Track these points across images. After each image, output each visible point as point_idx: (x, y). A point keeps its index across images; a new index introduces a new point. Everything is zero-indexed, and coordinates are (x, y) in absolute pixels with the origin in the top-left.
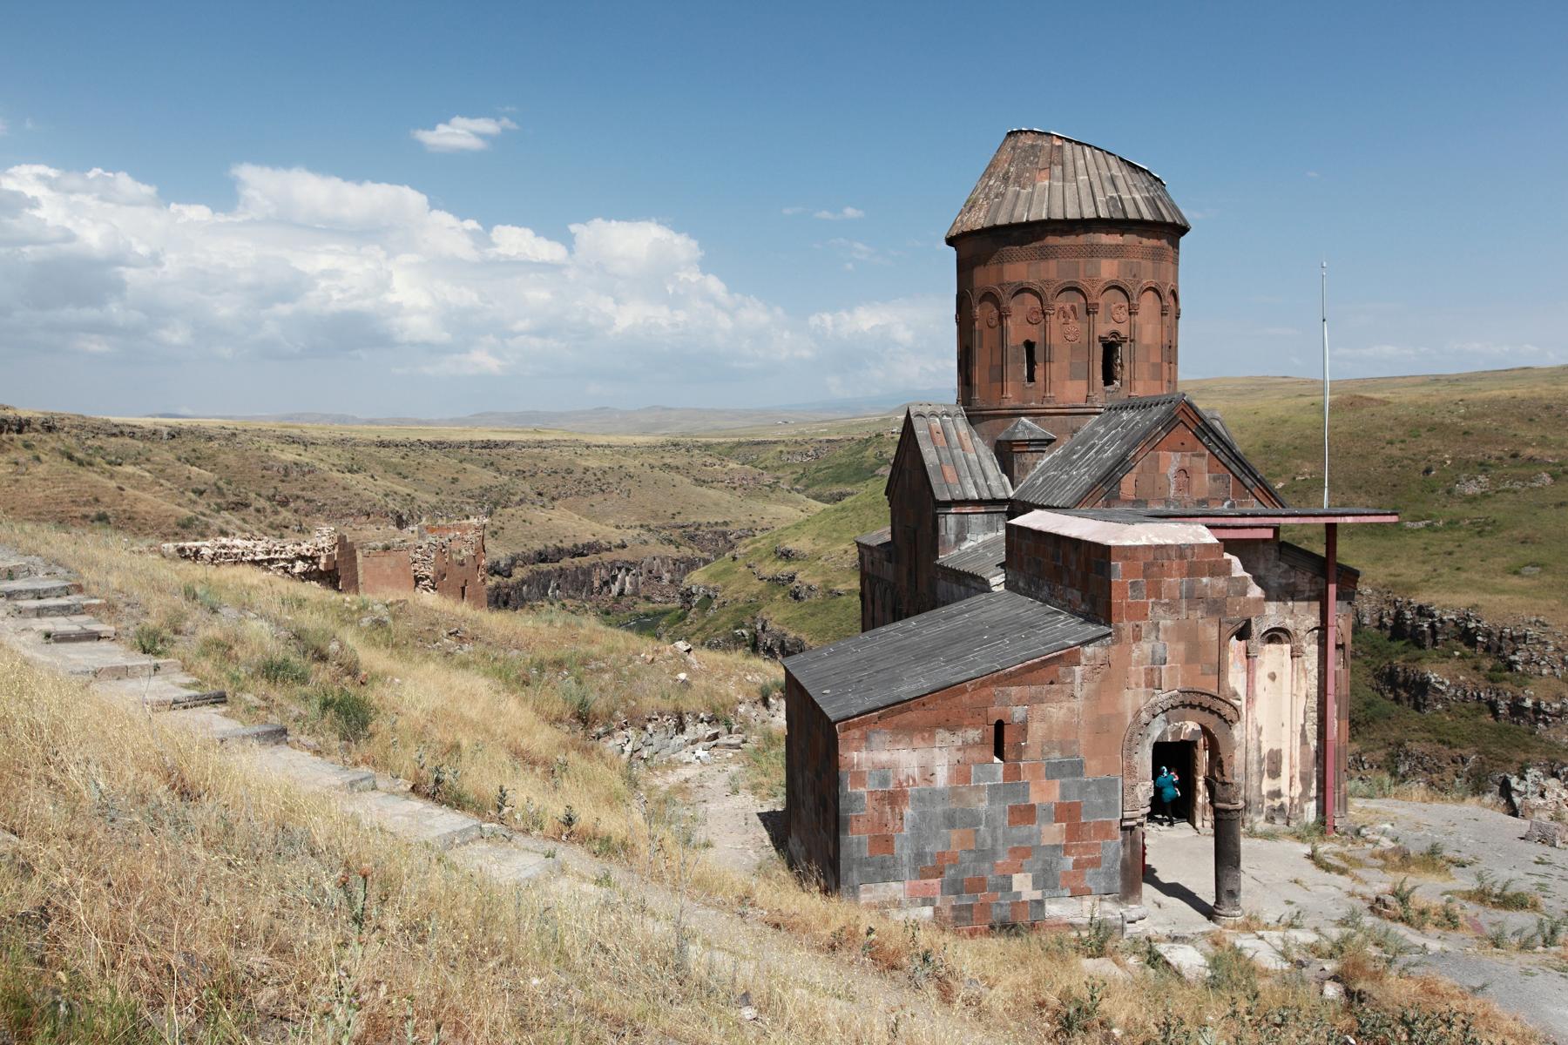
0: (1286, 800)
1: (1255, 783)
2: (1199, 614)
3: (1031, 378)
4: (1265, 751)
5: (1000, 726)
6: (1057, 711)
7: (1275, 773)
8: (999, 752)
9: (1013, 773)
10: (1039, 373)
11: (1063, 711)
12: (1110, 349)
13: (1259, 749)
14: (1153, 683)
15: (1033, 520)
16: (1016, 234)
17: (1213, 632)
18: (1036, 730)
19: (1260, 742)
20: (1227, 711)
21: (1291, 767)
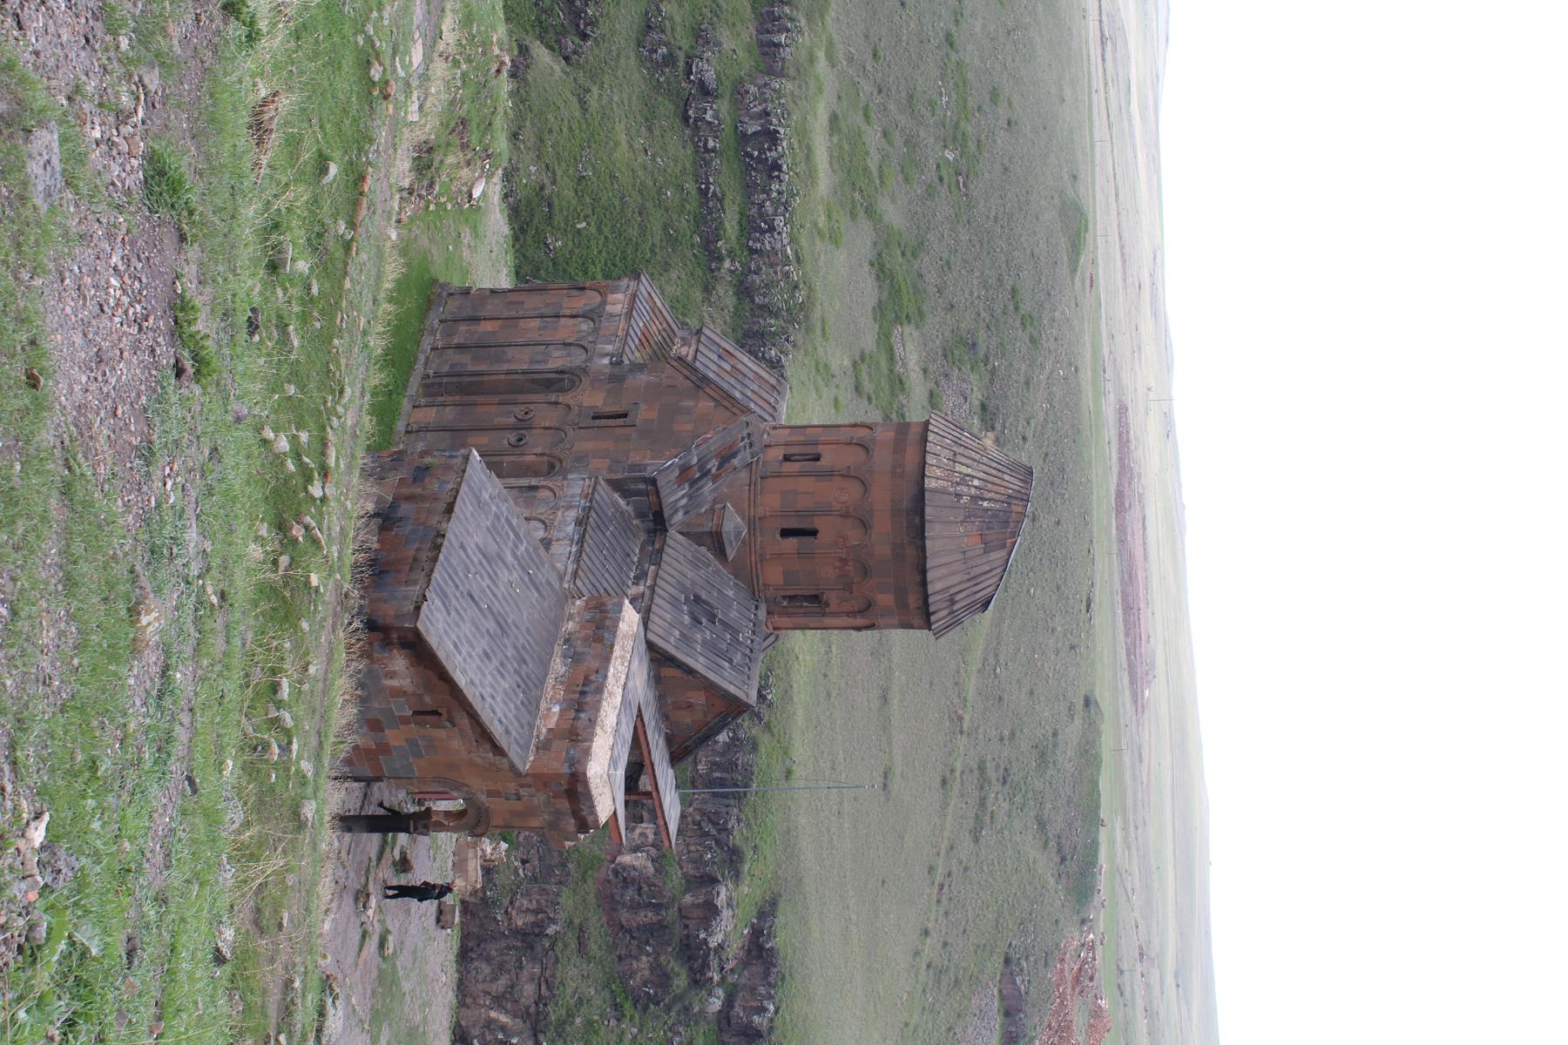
3: (785, 533)
5: (436, 713)
6: (456, 744)
8: (416, 713)
9: (405, 721)
10: (792, 543)
12: (815, 598)
14: (490, 794)
15: (630, 618)
16: (917, 520)
17: (535, 823)
18: (441, 734)
20: (479, 830)
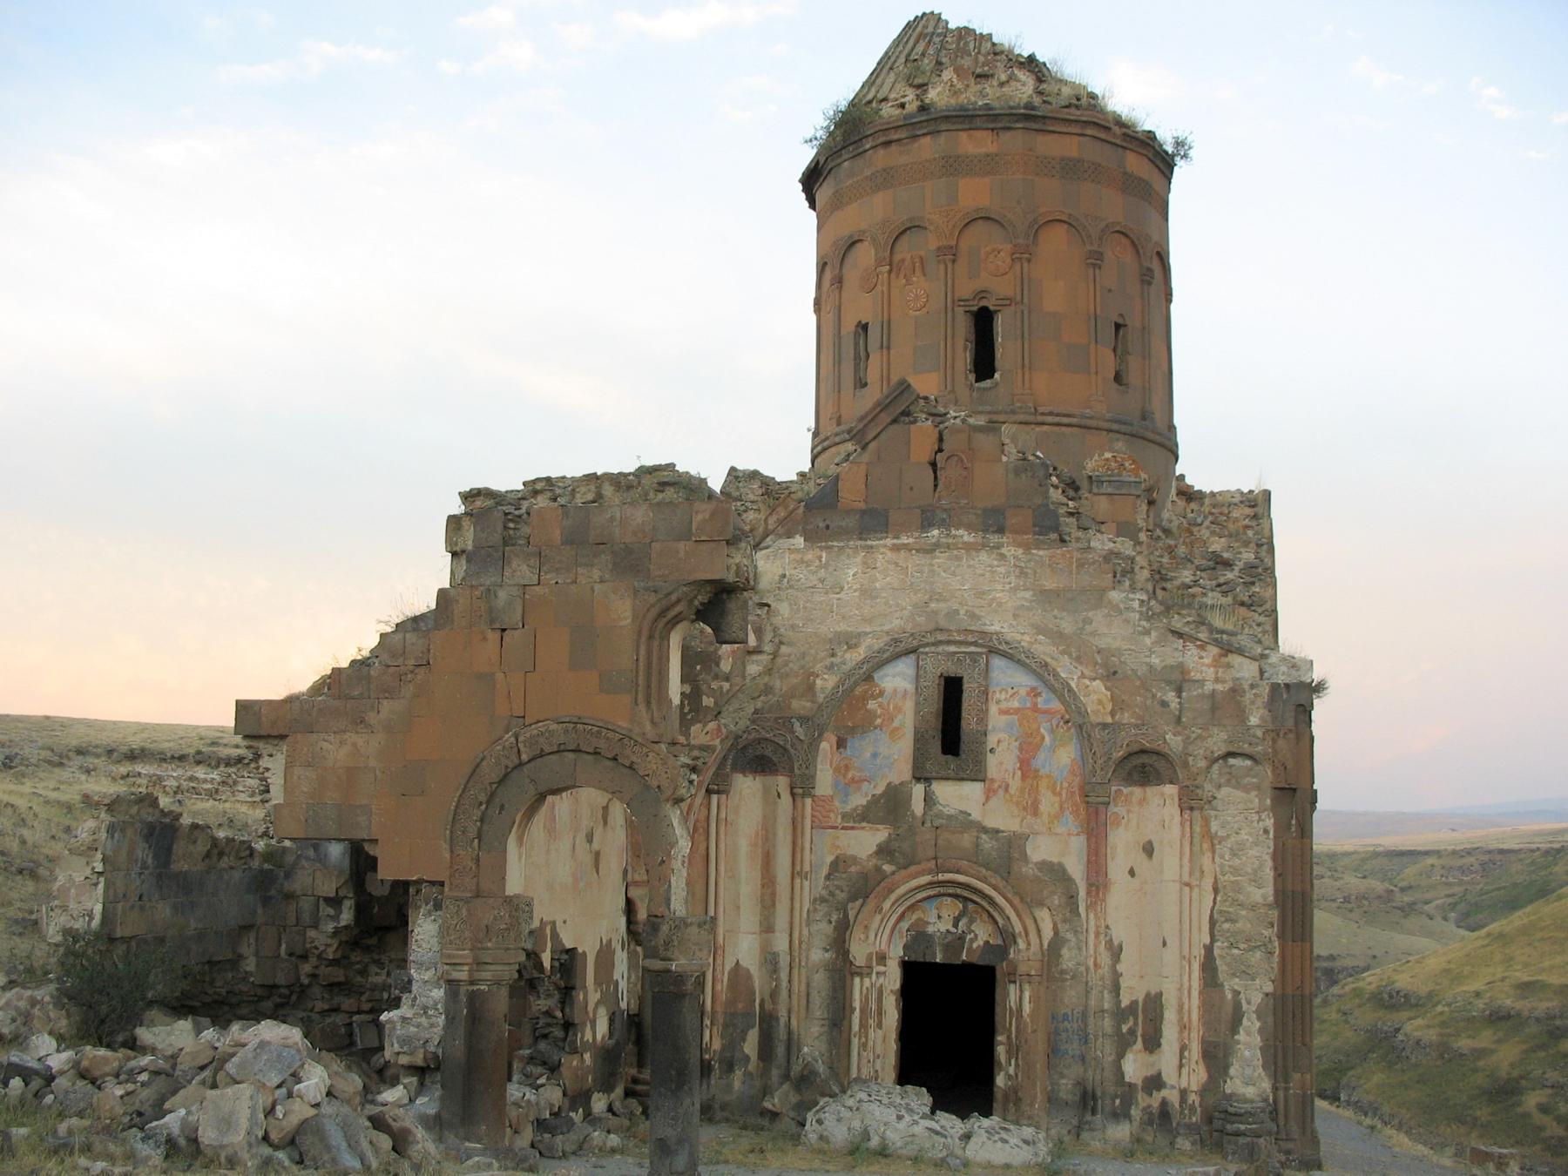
0: (1172, 1096)
1: (1104, 1050)
2: (596, 574)
4: (1133, 990)
7: (1153, 1043)
11: (345, 750)
12: (983, 321)
13: (1116, 989)
19: (1116, 976)
21: (1183, 1027)
